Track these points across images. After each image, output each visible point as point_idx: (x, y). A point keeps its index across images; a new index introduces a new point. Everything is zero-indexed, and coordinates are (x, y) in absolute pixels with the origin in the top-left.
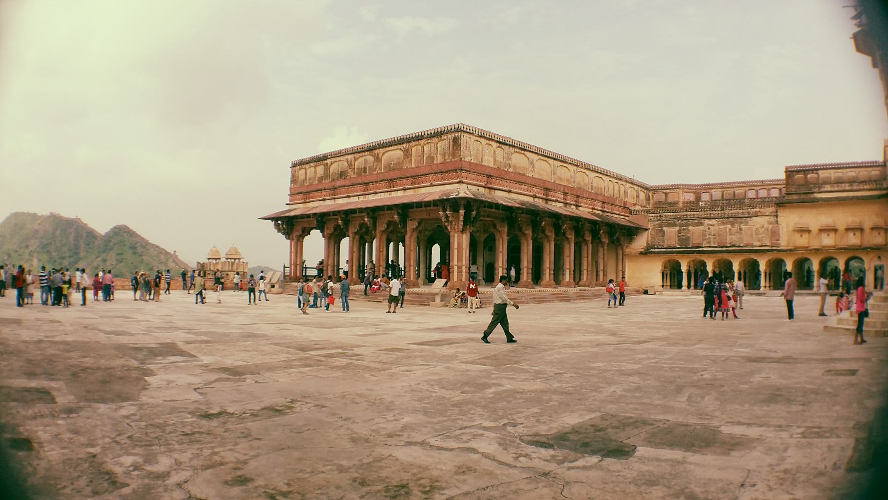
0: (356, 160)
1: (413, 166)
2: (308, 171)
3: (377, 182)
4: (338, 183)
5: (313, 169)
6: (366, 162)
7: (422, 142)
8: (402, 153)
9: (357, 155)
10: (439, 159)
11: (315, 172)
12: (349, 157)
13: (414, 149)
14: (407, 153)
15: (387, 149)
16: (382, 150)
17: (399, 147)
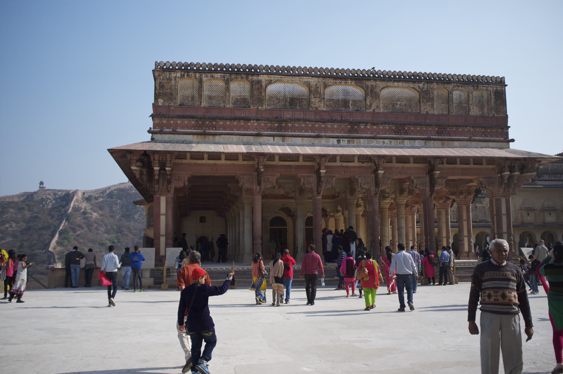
0: (326, 86)
1: (436, 112)
2: (206, 86)
3: (374, 124)
4: (288, 115)
5: (221, 84)
6: (346, 93)
7: (451, 87)
8: (414, 94)
9: (331, 81)
10: (475, 111)
11: (227, 89)
12: (313, 81)
13: (435, 92)
14: (425, 96)
15: (390, 84)
16: (380, 84)
17: (411, 85)
